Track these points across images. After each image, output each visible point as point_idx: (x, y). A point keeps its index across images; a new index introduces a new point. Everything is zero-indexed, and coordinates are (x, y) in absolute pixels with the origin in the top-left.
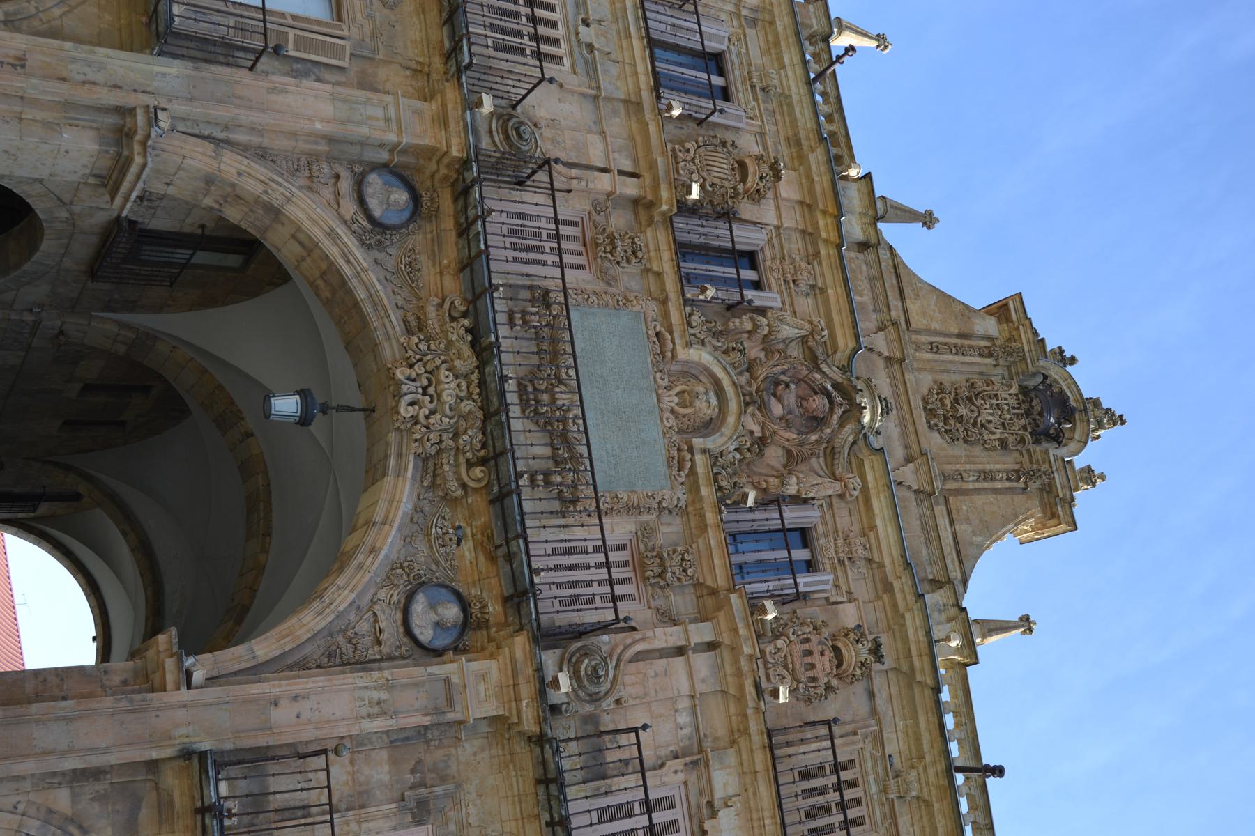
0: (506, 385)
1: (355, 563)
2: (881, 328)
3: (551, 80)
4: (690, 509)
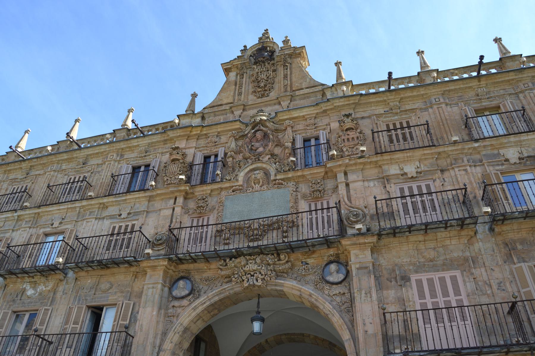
0: (251, 246)
1: (315, 302)
2: (233, 112)
3: (141, 228)
4: (296, 181)
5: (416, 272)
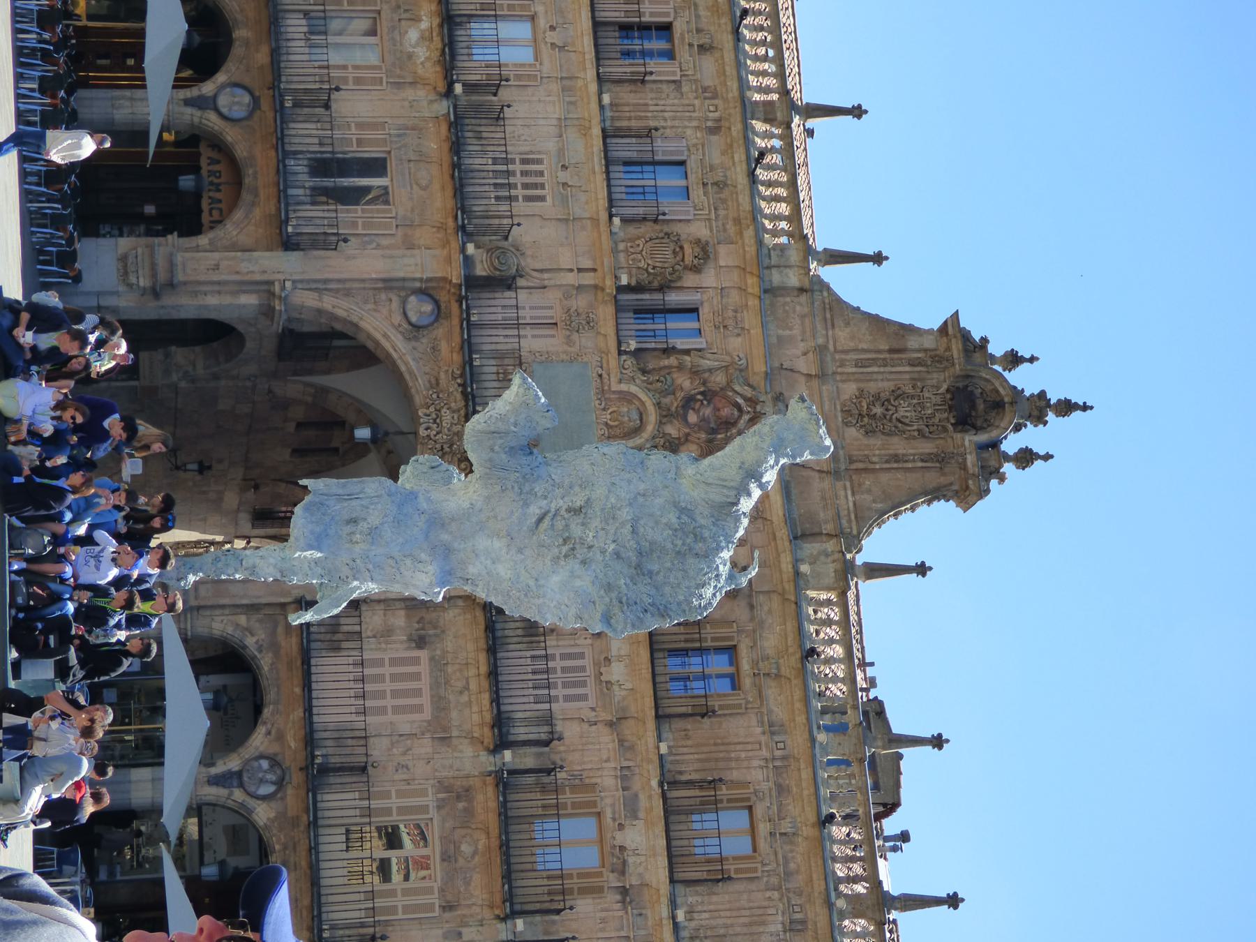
5: (432, 659)
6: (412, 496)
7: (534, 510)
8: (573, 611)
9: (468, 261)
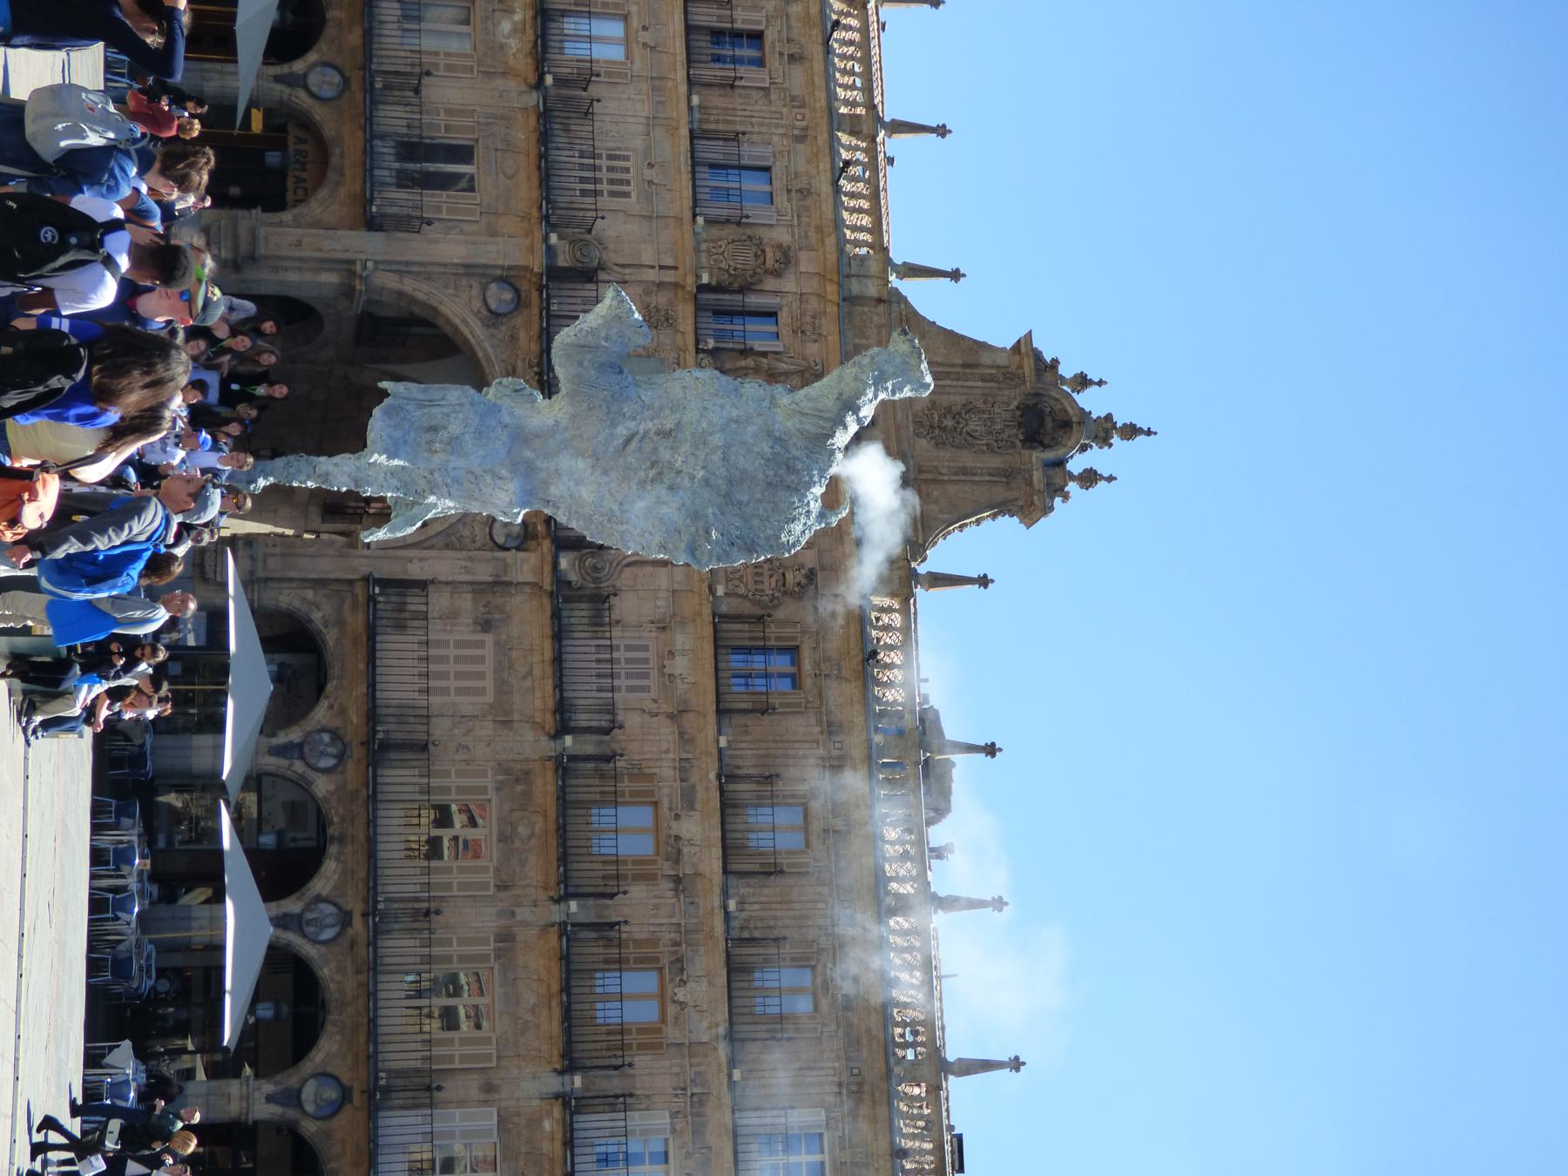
5: (497, 643)
6: (495, 409)
7: (622, 431)
8: (657, 539)
9: (550, 251)
